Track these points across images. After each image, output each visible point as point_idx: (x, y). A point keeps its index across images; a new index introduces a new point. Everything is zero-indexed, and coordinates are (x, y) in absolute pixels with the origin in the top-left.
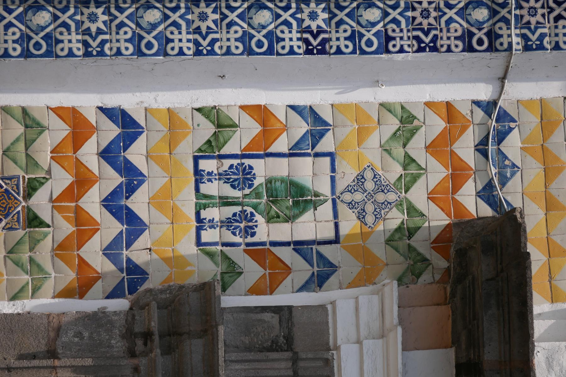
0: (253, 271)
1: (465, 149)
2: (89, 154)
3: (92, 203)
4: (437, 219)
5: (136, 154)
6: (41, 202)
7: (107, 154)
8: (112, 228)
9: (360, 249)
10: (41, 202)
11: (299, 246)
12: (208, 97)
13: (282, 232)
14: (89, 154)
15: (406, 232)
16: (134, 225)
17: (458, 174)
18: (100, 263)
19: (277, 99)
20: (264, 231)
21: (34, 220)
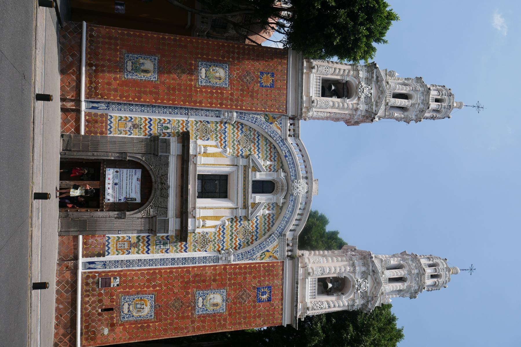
0: (163, 135)
1: (184, 124)
2: (147, 122)
3: (147, 127)
4: (181, 131)
5: (152, 122)
6: (142, 126)
7: (149, 122)
8: (149, 130)
9: (173, 133)
10: (142, 126)
11: (167, 133)
12: (159, 117)
13: (166, 131)
14: (147, 122)
15: (178, 132)
16: (151, 130)
17: (184, 127)
18: (148, 133)
19: (166, 118)
20: (164, 131)
21: (141, 128)
